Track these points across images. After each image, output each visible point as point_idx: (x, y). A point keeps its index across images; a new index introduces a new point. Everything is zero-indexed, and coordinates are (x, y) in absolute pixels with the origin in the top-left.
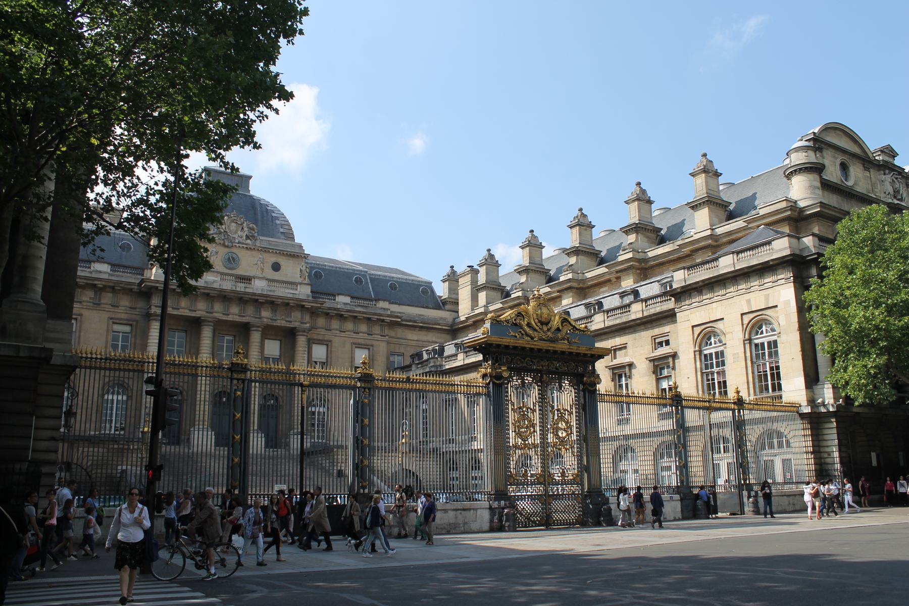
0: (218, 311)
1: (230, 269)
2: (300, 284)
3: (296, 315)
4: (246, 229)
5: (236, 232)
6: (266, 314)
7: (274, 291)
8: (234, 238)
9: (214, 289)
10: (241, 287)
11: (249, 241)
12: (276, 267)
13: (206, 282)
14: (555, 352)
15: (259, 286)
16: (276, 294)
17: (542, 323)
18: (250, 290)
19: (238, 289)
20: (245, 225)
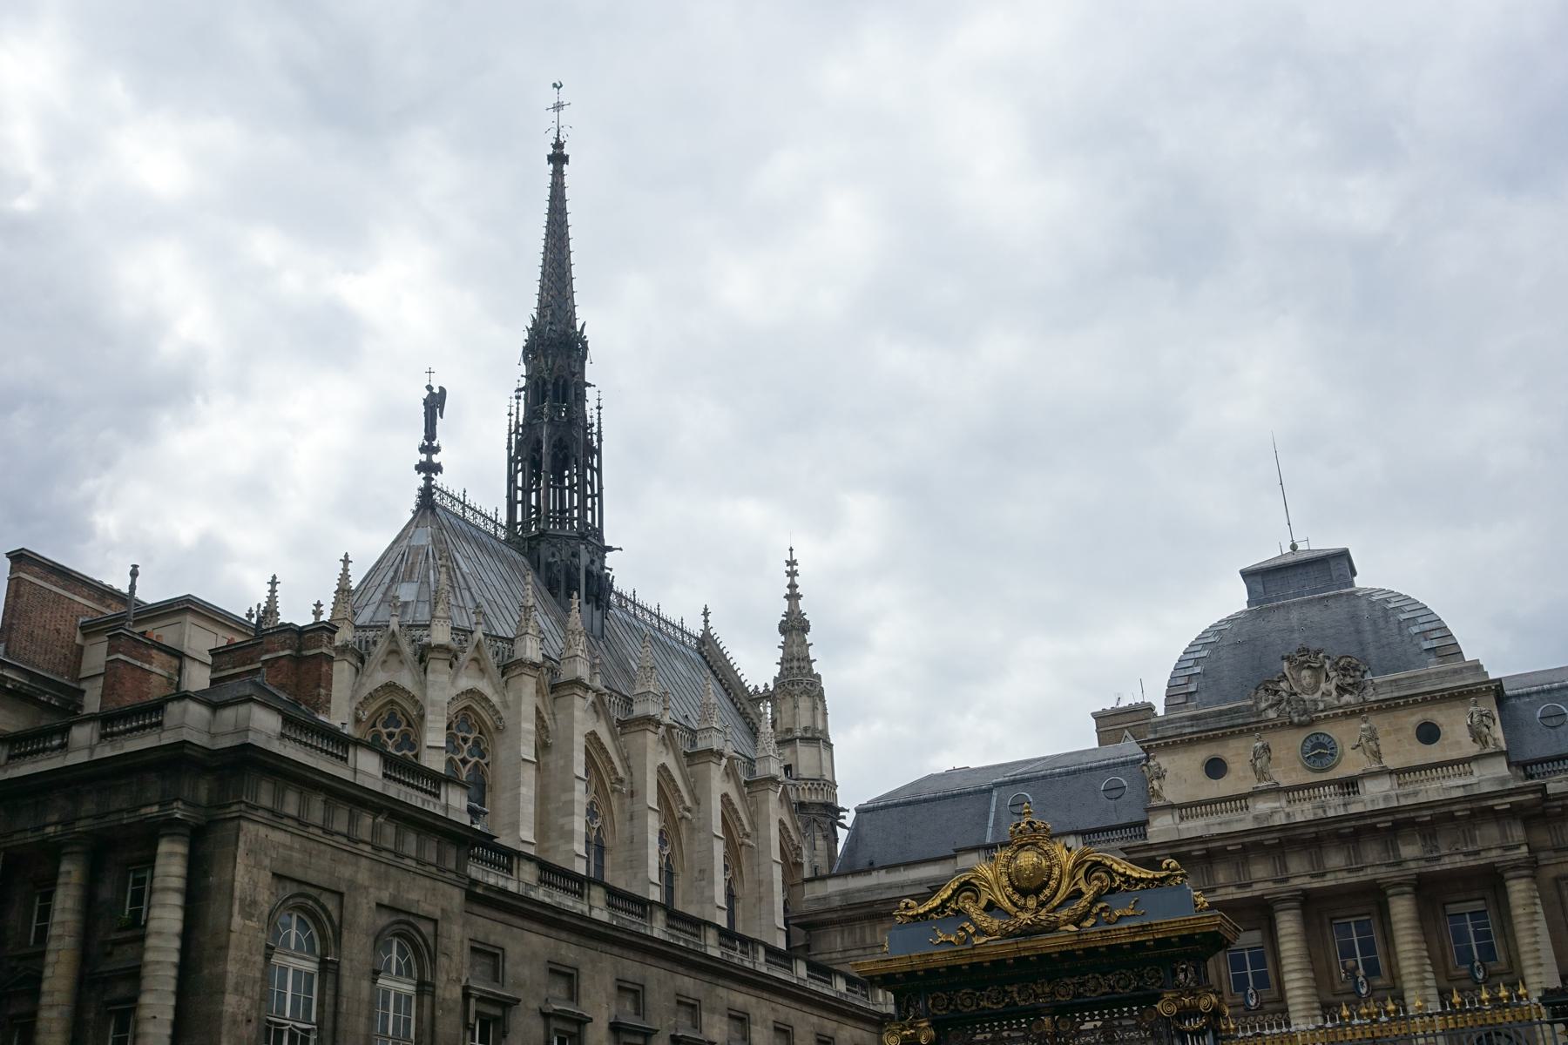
0: (1300, 874)
1: (1322, 771)
2: (1476, 758)
3: (1489, 834)
4: (1332, 674)
5: (1316, 688)
6: (1409, 850)
7: (1416, 793)
8: (1315, 702)
9: (1270, 829)
10: (1335, 806)
11: (1347, 698)
12: (1428, 734)
13: (1256, 818)
14: (1044, 958)
15: (1376, 794)
16: (1422, 799)
17: (1024, 893)
18: (1355, 809)
19: (1331, 813)
20: (1327, 666)
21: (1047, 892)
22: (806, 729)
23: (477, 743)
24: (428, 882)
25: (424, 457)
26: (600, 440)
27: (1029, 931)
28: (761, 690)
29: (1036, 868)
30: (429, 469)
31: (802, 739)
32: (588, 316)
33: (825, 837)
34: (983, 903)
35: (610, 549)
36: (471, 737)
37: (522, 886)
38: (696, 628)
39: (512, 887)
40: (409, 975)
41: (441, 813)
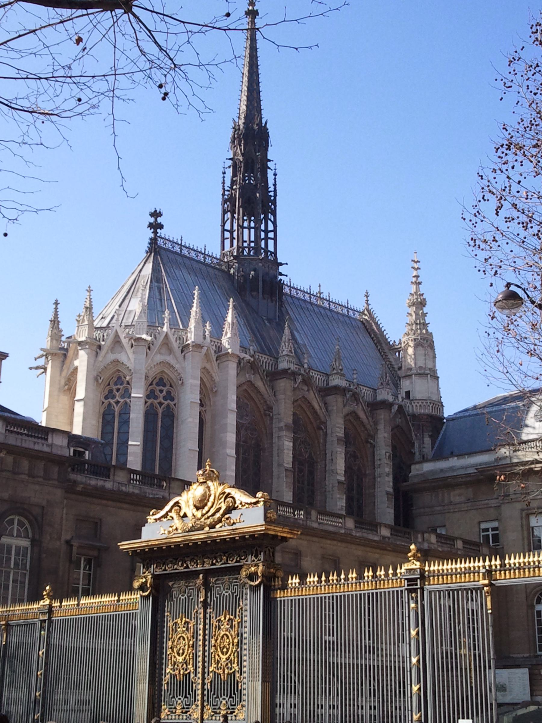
21: (206, 509)
22: (421, 368)
23: (169, 393)
24: (37, 487)
25: (152, 220)
26: (275, 195)
27: (193, 529)
28: (397, 343)
29: (204, 495)
30: (156, 226)
31: (415, 375)
32: (268, 114)
33: (430, 436)
34: (182, 514)
35: (281, 264)
36: (165, 389)
37: (116, 485)
38: (359, 304)
39: (109, 485)
40: (27, 537)
41: (46, 449)
